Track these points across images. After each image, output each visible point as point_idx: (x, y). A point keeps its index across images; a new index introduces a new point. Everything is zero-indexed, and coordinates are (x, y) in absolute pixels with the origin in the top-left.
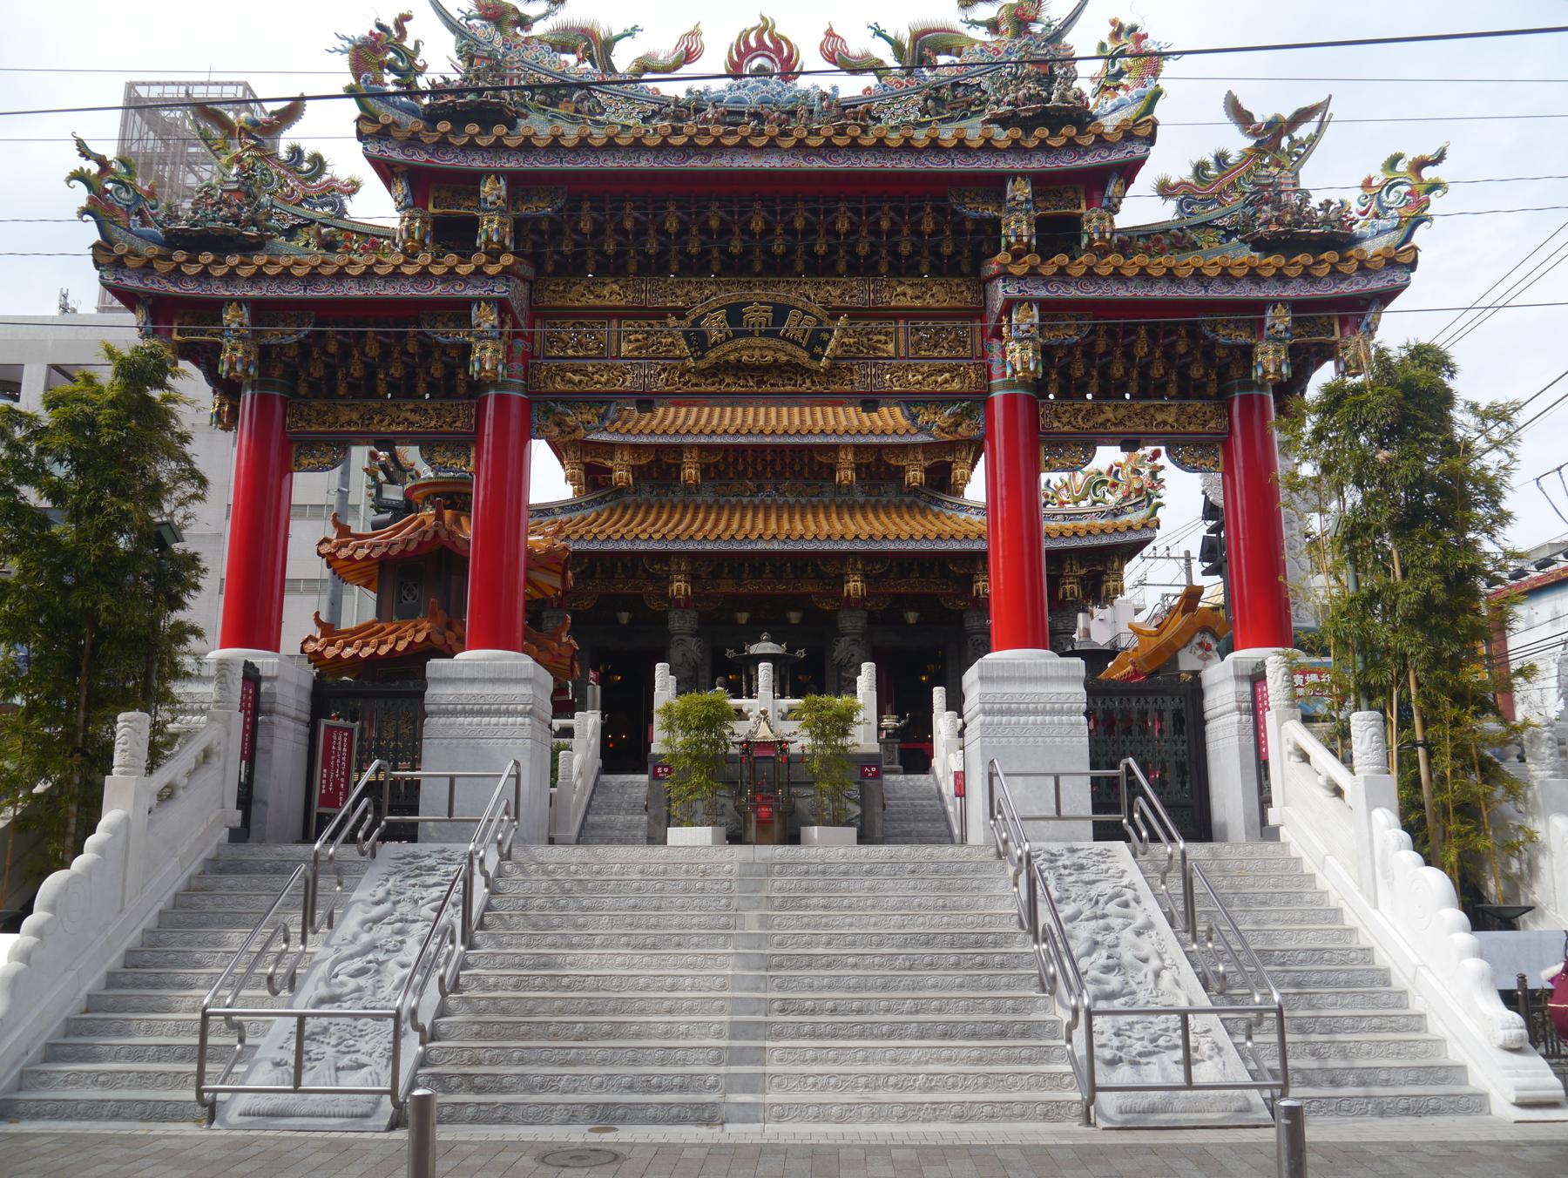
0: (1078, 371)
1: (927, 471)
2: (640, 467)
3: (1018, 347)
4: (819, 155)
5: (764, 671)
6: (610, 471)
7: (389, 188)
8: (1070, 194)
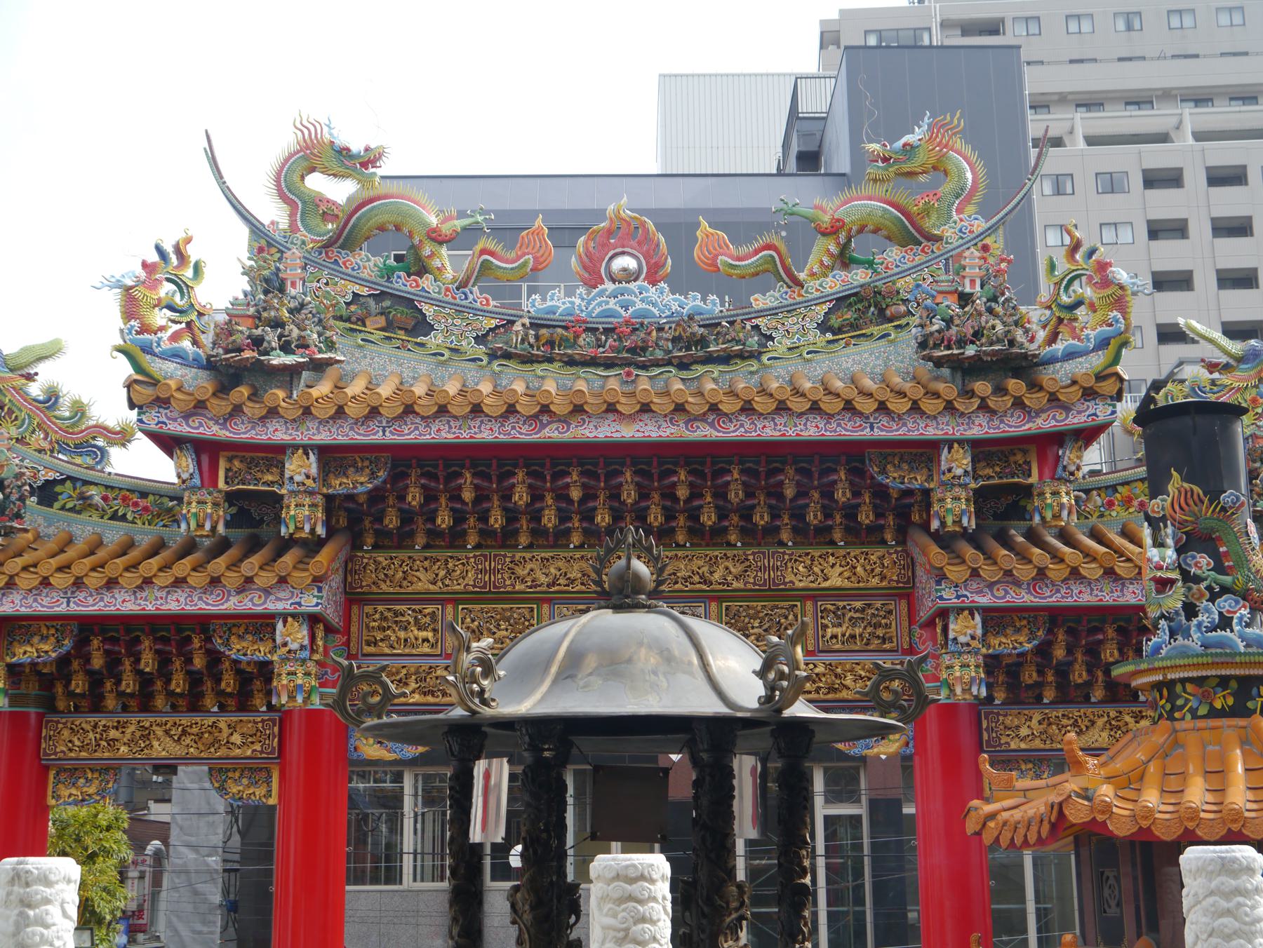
0: (1029, 676)
3: (957, 663)
4: (705, 421)
7: (171, 457)
8: (1019, 458)
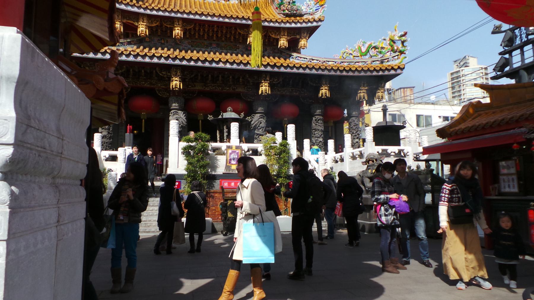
1: (289, 41)
2: (152, 27)
5: (235, 127)
6: (136, 28)
